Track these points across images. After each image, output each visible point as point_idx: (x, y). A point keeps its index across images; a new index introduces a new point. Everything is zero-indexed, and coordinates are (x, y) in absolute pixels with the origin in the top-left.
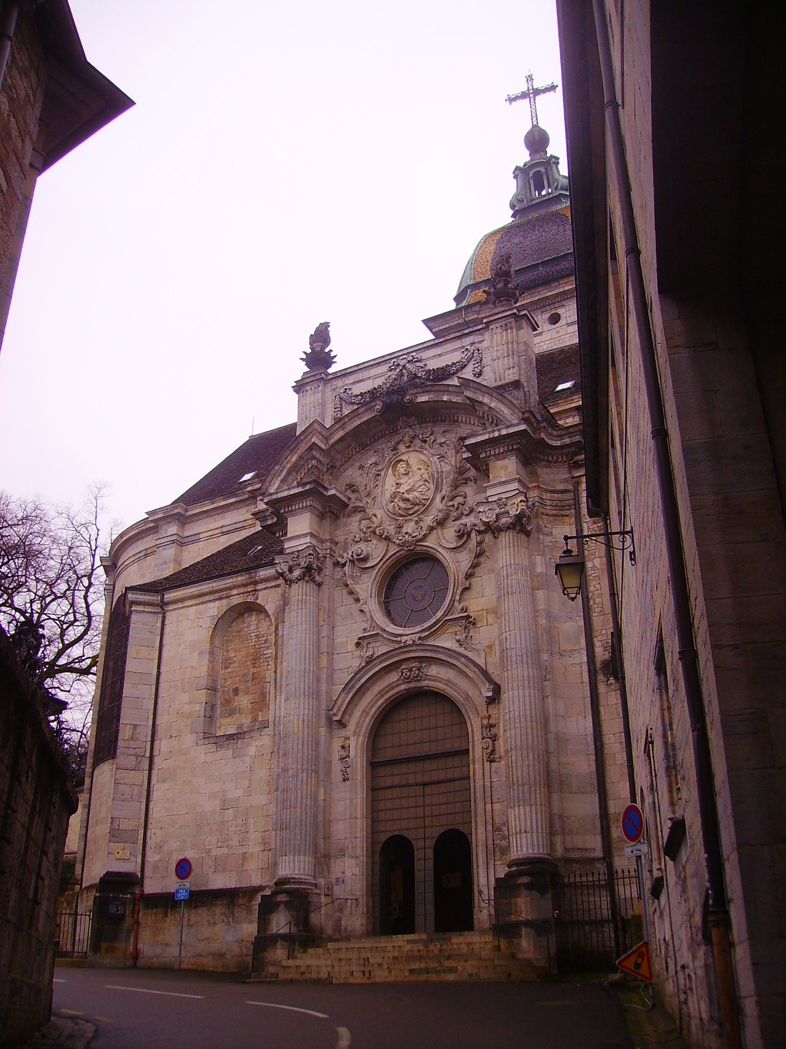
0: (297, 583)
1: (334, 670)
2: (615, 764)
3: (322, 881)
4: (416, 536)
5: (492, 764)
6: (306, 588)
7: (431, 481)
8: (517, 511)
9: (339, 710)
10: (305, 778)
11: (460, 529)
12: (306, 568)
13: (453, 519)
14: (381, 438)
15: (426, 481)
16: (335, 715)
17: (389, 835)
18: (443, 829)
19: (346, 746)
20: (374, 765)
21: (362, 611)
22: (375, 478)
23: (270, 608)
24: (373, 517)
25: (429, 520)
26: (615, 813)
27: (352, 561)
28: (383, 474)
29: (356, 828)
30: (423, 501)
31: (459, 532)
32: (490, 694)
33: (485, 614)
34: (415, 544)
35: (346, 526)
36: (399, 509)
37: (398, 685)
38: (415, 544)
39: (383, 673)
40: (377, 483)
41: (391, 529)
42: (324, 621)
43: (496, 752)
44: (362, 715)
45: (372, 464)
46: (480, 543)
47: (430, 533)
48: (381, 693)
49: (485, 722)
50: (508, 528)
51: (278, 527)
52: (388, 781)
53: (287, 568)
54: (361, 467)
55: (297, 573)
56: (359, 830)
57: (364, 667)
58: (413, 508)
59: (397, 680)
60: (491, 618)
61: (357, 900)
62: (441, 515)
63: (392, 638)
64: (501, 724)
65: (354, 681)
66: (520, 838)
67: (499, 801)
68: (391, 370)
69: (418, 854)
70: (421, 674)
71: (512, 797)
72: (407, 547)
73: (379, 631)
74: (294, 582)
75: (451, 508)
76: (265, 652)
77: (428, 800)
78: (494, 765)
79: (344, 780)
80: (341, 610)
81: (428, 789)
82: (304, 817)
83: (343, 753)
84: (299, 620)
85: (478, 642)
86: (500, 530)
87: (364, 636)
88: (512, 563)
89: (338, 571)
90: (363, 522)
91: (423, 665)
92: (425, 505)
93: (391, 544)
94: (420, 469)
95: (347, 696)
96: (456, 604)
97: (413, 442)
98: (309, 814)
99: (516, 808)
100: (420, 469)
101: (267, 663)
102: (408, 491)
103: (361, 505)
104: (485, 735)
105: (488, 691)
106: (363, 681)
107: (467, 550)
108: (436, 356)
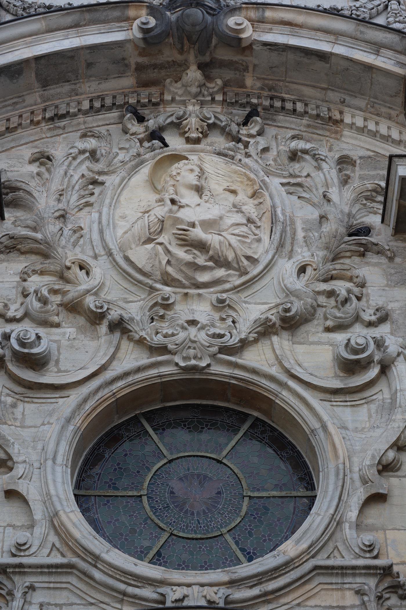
4: (221, 336)
7: (265, 224)
11: (363, 351)
13: (330, 323)
14: (110, 109)
15: (250, 221)
22: (84, 187)
28: (111, 180)
30: (245, 262)
31: (356, 352)
34: (213, 356)
36: (169, 262)
38: (213, 356)
40: (92, 199)
45: (82, 152)
47: (256, 341)
58: (211, 269)
62: (296, 306)
63: (122, 587)
72: (185, 359)
73: (75, 560)
75: (322, 299)
87: (21, 565)
92: (247, 273)
93: (126, 346)
94: (234, 192)
96: (348, 532)
97: (205, 136)
100: (234, 192)
103: (39, 236)
107: (373, 407)
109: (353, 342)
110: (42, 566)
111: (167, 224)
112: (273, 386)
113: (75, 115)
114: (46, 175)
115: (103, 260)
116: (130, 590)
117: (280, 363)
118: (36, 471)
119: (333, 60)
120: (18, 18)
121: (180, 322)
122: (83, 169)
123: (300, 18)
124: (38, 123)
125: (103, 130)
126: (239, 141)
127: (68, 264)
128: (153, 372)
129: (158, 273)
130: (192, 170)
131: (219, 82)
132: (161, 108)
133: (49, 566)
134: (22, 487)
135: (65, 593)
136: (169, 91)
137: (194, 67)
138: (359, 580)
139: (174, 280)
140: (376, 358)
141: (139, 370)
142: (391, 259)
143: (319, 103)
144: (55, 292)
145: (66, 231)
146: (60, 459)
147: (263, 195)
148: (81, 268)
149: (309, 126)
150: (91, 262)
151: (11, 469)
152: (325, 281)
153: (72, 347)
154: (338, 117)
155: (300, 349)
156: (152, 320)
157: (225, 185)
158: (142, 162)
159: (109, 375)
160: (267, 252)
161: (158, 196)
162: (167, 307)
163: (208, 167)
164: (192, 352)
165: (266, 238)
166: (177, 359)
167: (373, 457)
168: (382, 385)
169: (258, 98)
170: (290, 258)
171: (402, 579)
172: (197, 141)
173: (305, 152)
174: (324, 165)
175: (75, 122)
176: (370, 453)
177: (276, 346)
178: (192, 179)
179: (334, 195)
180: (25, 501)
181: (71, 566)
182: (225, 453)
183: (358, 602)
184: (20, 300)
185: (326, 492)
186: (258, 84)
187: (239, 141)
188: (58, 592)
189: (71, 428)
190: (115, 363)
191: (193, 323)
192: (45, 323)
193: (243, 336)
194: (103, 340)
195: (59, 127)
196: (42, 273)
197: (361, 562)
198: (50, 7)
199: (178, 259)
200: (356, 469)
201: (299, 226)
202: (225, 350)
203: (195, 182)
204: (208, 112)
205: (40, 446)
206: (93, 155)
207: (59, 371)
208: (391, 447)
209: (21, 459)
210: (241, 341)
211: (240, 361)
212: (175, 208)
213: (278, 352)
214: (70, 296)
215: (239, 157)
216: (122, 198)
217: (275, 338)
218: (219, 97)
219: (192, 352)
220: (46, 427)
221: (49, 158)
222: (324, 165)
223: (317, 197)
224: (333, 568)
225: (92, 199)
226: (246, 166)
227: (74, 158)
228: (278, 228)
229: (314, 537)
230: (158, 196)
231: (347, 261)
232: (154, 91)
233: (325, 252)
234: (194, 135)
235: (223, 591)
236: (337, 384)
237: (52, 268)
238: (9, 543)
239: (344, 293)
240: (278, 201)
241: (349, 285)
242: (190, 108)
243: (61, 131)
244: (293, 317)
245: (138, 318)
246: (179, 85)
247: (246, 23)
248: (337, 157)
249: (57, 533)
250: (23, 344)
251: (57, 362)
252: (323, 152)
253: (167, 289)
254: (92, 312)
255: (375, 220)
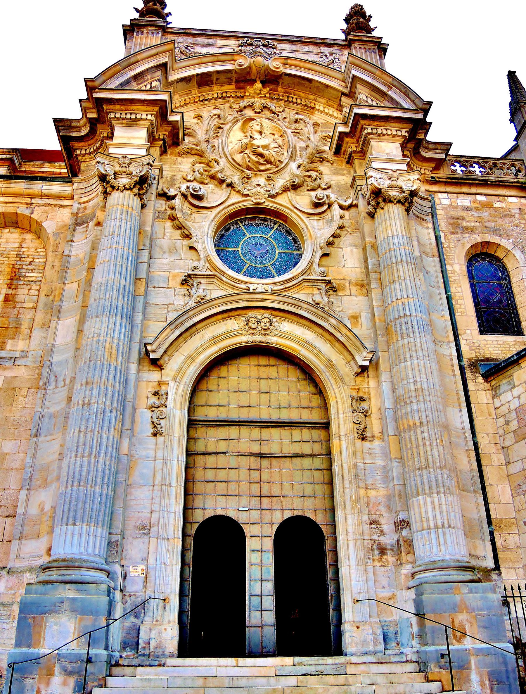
0: (122, 191)
1: (147, 303)
2: (492, 465)
3: (117, 569)
4: (269, 191)
5: (364, 442)
6: (133, 200)
7: (285, 148)
8: (412, 186)
9: (159, 347)
10: (113, 421)
11: (322, 199)
12: (141, 177)
13: (309, 188)
15: (280, 146)
16: (154, 351)
17: (210, 514)
18: (288, 515)
19: (163, 392)
20: (192, 423)
21: (191, 248)
22: (215, 130)
23: (49, 226)
24: (213, 162)
25: (281, 182)
26: (496, 518)
27: (184, 196)
28: (226, 127)
29: (169, 499)
30: (278, 163)
31: (319, 199)
32: (366, 363)
33: (347, 285)
34: (266, 198)
35: (175, 164)
36: (249, 161)
37: (238, 335)
39: (220, 317)
40: (219, 135)
41: (236, 178)
42: (144, 245)
43: (367, 429)
44: (186, 361)
45: (215, 115)
46: (341, 217)
47: (282, 193)
48: (215, 340)
49: (354, 394)
50: (399, 202)
51: (81, 144)
52: (211, 447)
53: (113, 172)
54: (199, 117)
55: (124, 181)
56: (173, 501)
57: (191, 309)
58: (265, 164)
59: (238, 330)
60: (355, 290)
61: (164, 600)
62: (297, 181)
63: (234, 284)
64: (373, 400)
65: (185, 317)
66: (444, 533)
67: (374, 487)
68: (242, 46)
69: (251, 544)
70: (271, 328)
71: (426, 481)
72: (255, 199)
73: (216, 273)
74: (118, 189)
75: (306, 178)
76: (28, 275)
77: (265, 476)
78: (367, 444)
79: (155, 435)
80: (165, 243)
81: (265, 463)
82: (107, 472)
83: (153, 400)
84: (122, 230)
85: (341, 310)
86: (388, 200)
87: (196, 275)
88: (404, 234)
89: (162, 204)
90: (197, 165)
91: (274, 320)
92: (278, 167)
94: (273, 134)
95: (172, 333)
96: (315, 266)
97: (262, 111)
98: (113, 469)
99: (435, 495)
100: (273, 134)
101: (29, 287)
102: (265, 147)
103: (199, 148)
104: (356, 408)
105: (363, 360)
106: (196, 319)
107: (325, 221)
108: (291, 50)
109: (318, 196)
110: (204, 275)
111: (249, 146)
112: (288, 211)
113: (211, 99)
114: (200, 124)
115: (224, 159)
116: (236, 285)
117: (290, 202)
118: (200, 240)
119: (313, 82)
120: (188, 58)
121: (254, 185)
122: (215, 122)
123: (302, 64)
124: (197, 102)
125: (222, 107)
126: (275, 113)
127: (210, 160)
128: (243, 204)
129: (245, 165)
130: (258, 125)
131: (268, 89)
132: (245, 99)
133: (206, 275)
134: (195, 245)
135: (212, 285)
136: (248, 92)
137: (258, 82)
138: (319, 284)
139: (251, 168)
140: (327, 202)
141: (238, 203)
142: (332, 164)
143: (306, 100)
144: (206, 171)
145: (209, 147)
146: (209, 236)
147: (285, 136)
148: (216, 162)
149: (302, 109)
150: (219, 159)
151: (191, 239)
152: (308, 171)
153: (212, 192)
154: (313, 106)
155: (298, 197)
156: (243, 183)
157: (270, 131)
158: (238, 120)
159: (227, 204)
160: (286, 159)
161: (244, 135)
162: (248, 179)
163: (264, 124)
164: (258, 197)
165: (285, 153)
166: (252, 199)
167: (325, 239)
168: (328, 212)
169: (283, 96)
170: (295, 162)
171: (334, 285)
172: (259, 113)
173: (301, 119)
174: (308, 125)
175: (211, 102)
176: (323, 238)
177: (289, 196)
178: (258, 128)
179: (311, 137)
180: (196, 250)
181: (215, 276)
182: (269, 235)
183: (318, 293)
184: (192, 173)
185: (307, 251)
186: (283, 91)
187: (275, 113)
188: (209, 285)
189: (213, 224)
190: (229, 199)
191: (258, 185)
192: (202, 183)
193: (277, 191)
194: (224, 190)
195: (205, 104)
196: (200, 163)
197: (320, 278)
198: (200, 53)
199: (252, 160)
200: (318, 244)
201: (298, 149)
202: (271, 196)
203: (259, 130)
204: (263, 101)
205: (202, 230)
206: (219, 116)
207: (208, 202)
208: (331, 236)
209: (195, 235)
210: (276, 193)
211: (276, 201)
212: (252, 139)
213: (290, 198)
214: (211, 173)
215: (275, 120)
216: (230, 135)
217: (289, 193)
218: (268, 95)
219: (258, 197)
220: (204, 223)
221: (201, 117)
222: (308, 125)
223: (305, 138)
224: (310, 280)
225: (219, 135)
226: (278, 124)
227: (212, 117)
228: (290, 150)
229: (303, 268)
230: (244, 135)
231: (316, 164)
232: (242, 90)
233: (308, 160)
234: (258, 111)
235: (270, 287)
236: (311, 211)
237: (204, 161)
238: (191, 266)
239: (314, 177)
240: (290, 139)
241: (317, 173)
242: (256, 99)
243: (205, 106)
244: (295, 185)
245: (237, 182)
246: (252, 89)
247: (280, 64)
248: (313, 122)
249: (210, 264)
250: (195, 191)
251: (207, 198)
252: (307, 120)
253: (248, 172)
254: (220, 179)
255: (327, 148)
